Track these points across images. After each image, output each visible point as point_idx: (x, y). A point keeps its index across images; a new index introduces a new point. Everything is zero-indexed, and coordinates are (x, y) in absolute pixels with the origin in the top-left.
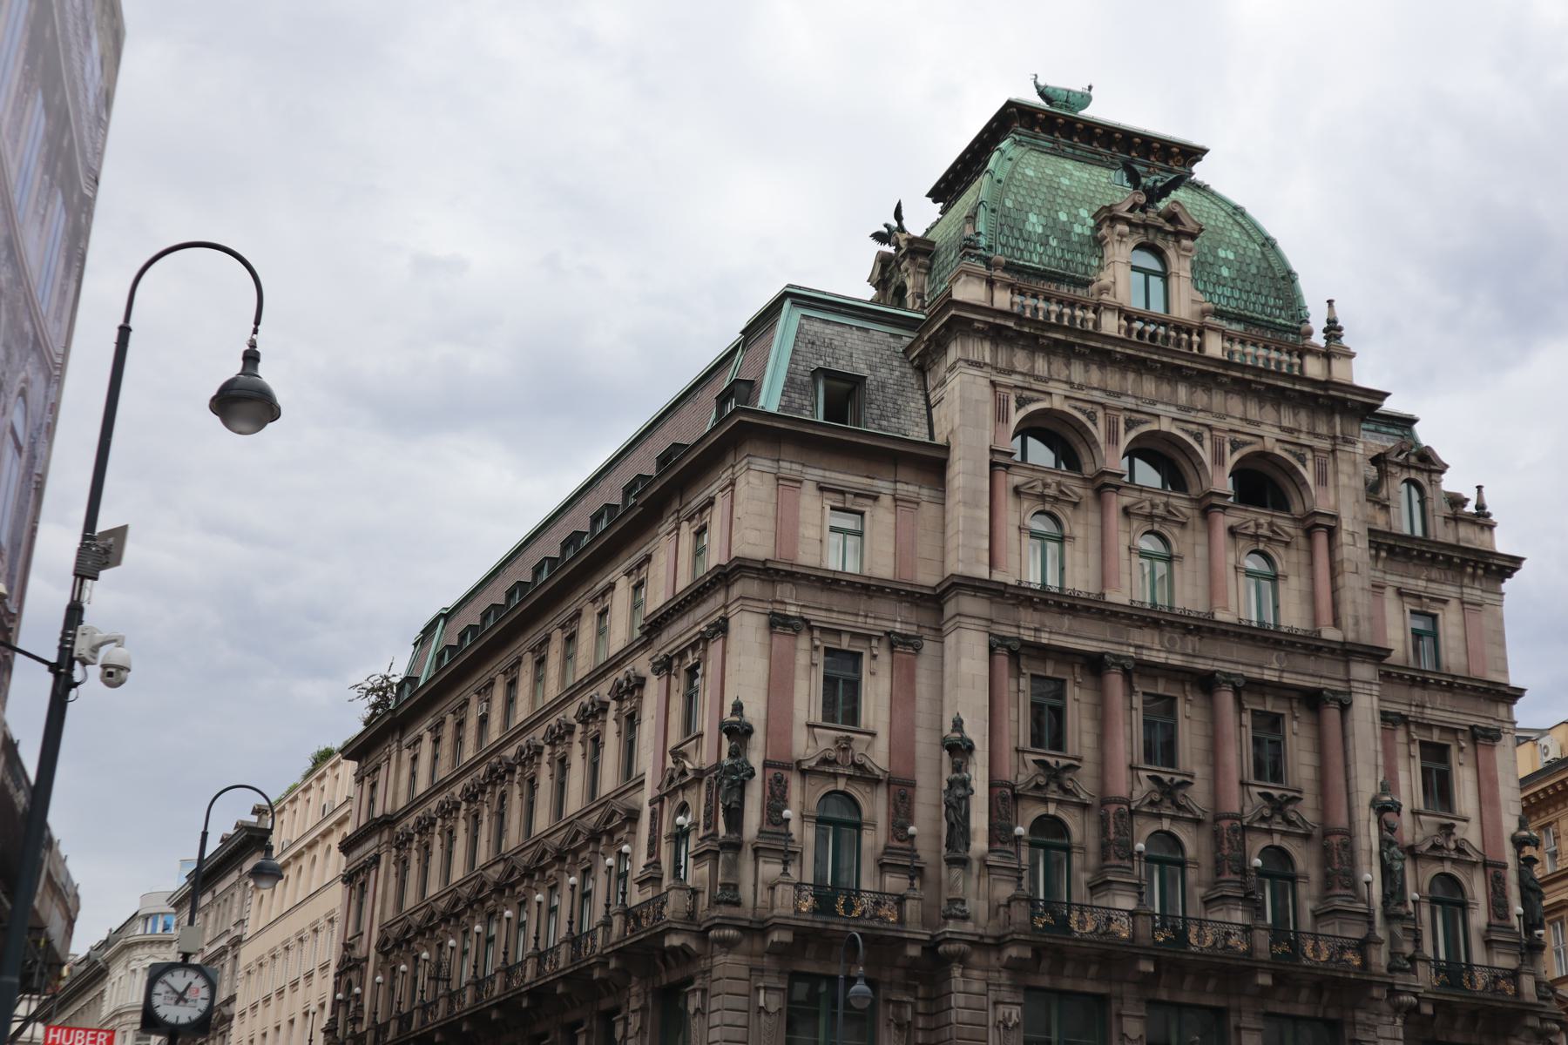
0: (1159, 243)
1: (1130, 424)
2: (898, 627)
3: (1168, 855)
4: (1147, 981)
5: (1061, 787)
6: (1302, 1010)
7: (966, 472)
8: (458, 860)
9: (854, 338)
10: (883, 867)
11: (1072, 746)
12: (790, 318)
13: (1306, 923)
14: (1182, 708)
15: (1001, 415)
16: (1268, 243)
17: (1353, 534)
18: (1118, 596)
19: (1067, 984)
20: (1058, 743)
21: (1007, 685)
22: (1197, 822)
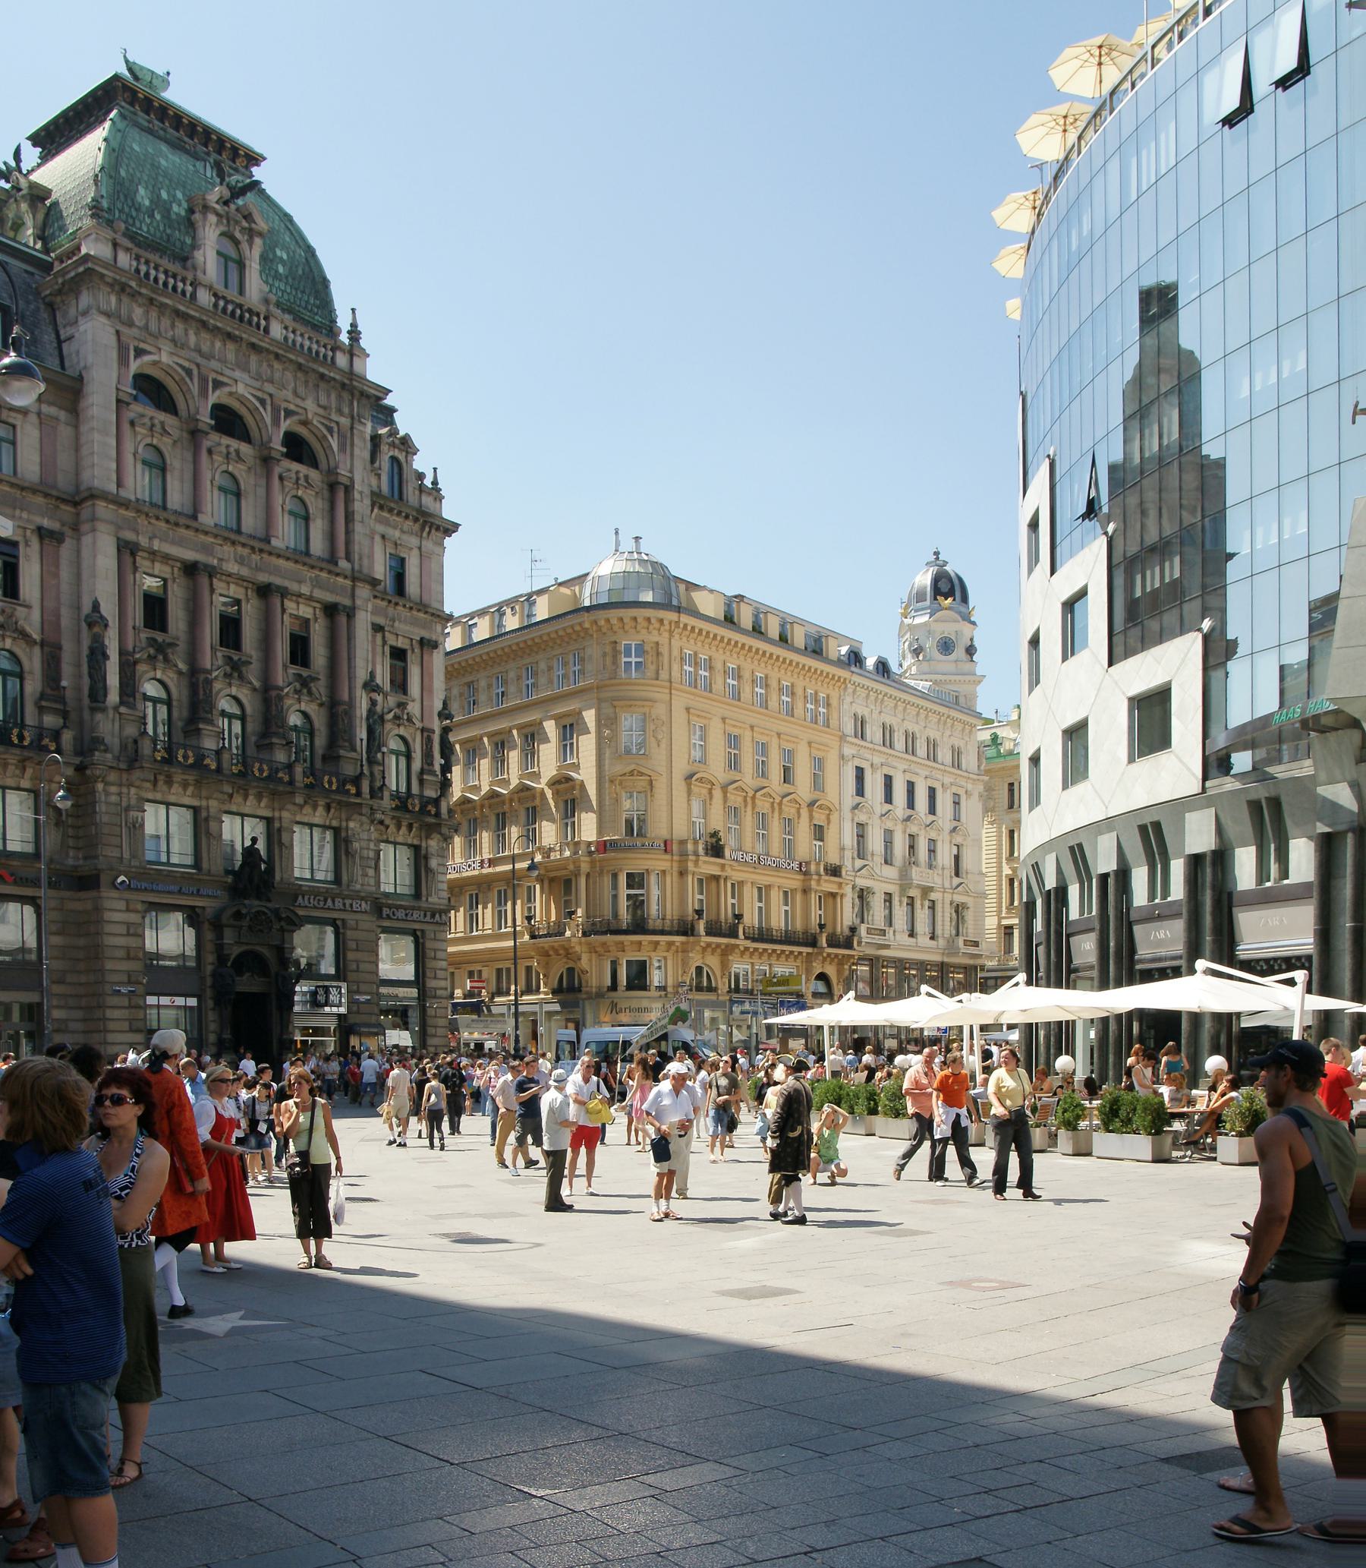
0: (238, 235)
2: (46, 523)
5: (166, 660)
6: (317, 820)
17: (361, 493)
20: (163, 628)
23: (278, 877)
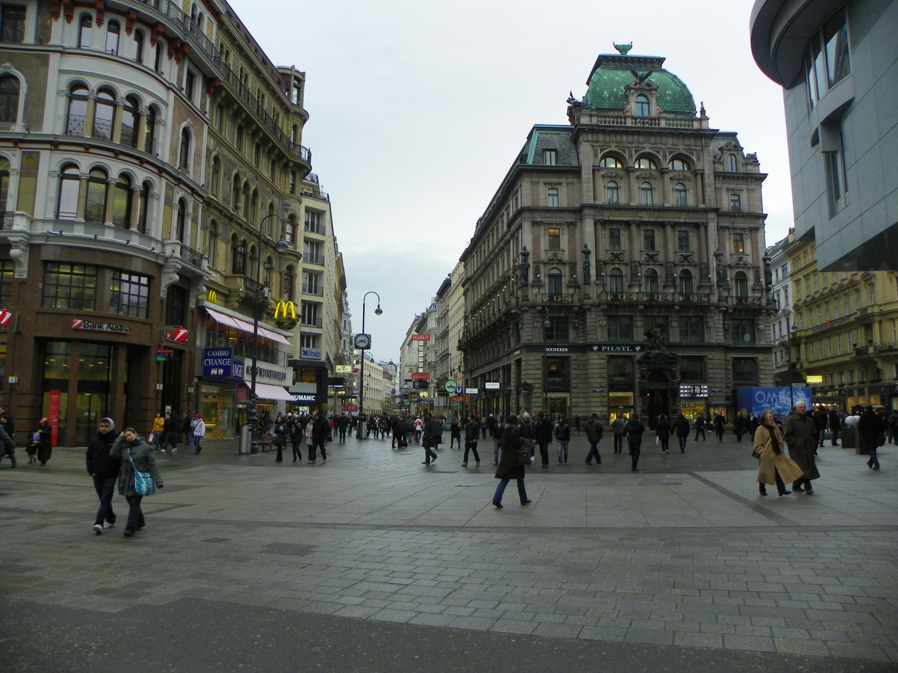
0: (645, 93)
1: (636, 152)
2: (569, 220)
3: (652, 277)
4: (642, 311)
6: (691, 314)
7: (586, 173)
8: (482, 289)
9: (555, 137)
10: (568, 287)
11: (623, 248)
12: (536, 135)
13: (695, 290)
14: (656, 233)
15: (596, 155)
16: (684, 86)
18: (633, 204)
19: (620, 314)
21: (601, 232)
22: (661, 265)
23: (671, 340)
